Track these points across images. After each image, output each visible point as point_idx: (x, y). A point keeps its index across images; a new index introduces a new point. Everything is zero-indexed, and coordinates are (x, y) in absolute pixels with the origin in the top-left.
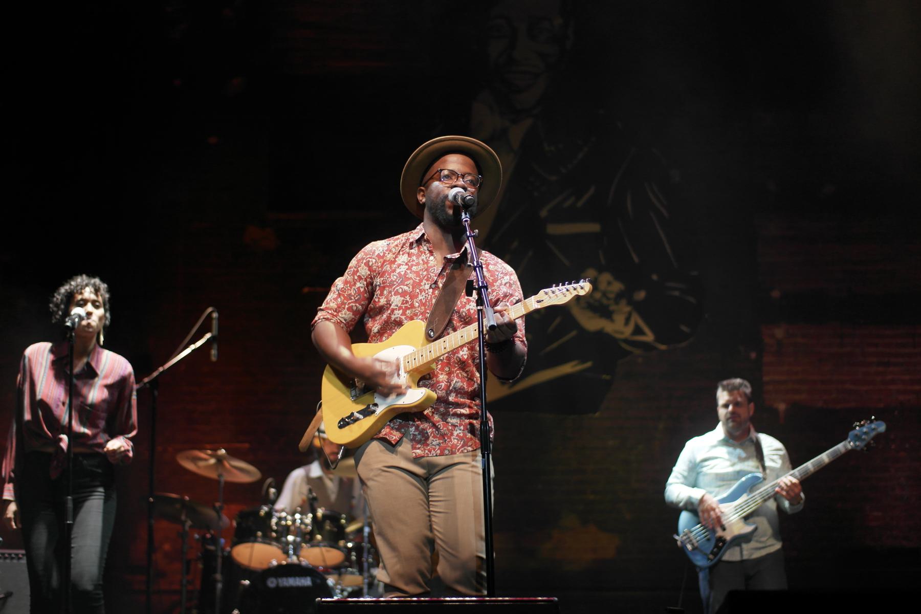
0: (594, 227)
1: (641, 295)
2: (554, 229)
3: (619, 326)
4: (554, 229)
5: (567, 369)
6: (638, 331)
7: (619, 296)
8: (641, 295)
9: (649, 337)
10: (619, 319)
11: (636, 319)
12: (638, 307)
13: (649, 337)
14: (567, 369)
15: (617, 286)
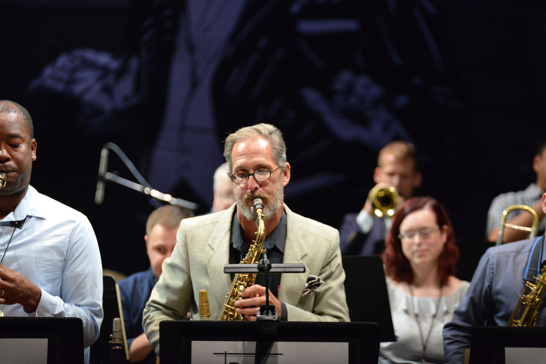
1: (402, 101)
8: (402, 101)
15: (375, 91)
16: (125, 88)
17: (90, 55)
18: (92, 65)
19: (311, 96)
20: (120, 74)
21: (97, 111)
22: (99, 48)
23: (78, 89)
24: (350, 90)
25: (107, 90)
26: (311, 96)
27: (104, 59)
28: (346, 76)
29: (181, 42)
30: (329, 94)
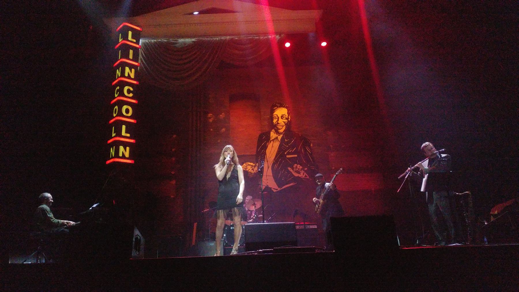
0: (296, 156)
1: (306, 169)
2: (288, 156)
3: (302, 175)
4: (288, 156)
5: (291, 184)
6: (306, 176)
7: (302, 169)
8: (306, 169)
9: (308, 177)
10: (302, 174)
11: (305, 173)
12: (306, 171)
13: (308, 177)
14: (291, 184)
15: (301, 167)
16: (256, 169)
17: (249, 163)
18: (250, 165)
19: (289, 169)
20: (255, 166)
21: (252, 173)
22: (250, 162)
23: (247, 169)
24: (296, 167)
25: (253, 169)
26: (289, 169)
27: (252, 164)
28: (296, 165)
29: (266, 160)
30: (293, 169)
